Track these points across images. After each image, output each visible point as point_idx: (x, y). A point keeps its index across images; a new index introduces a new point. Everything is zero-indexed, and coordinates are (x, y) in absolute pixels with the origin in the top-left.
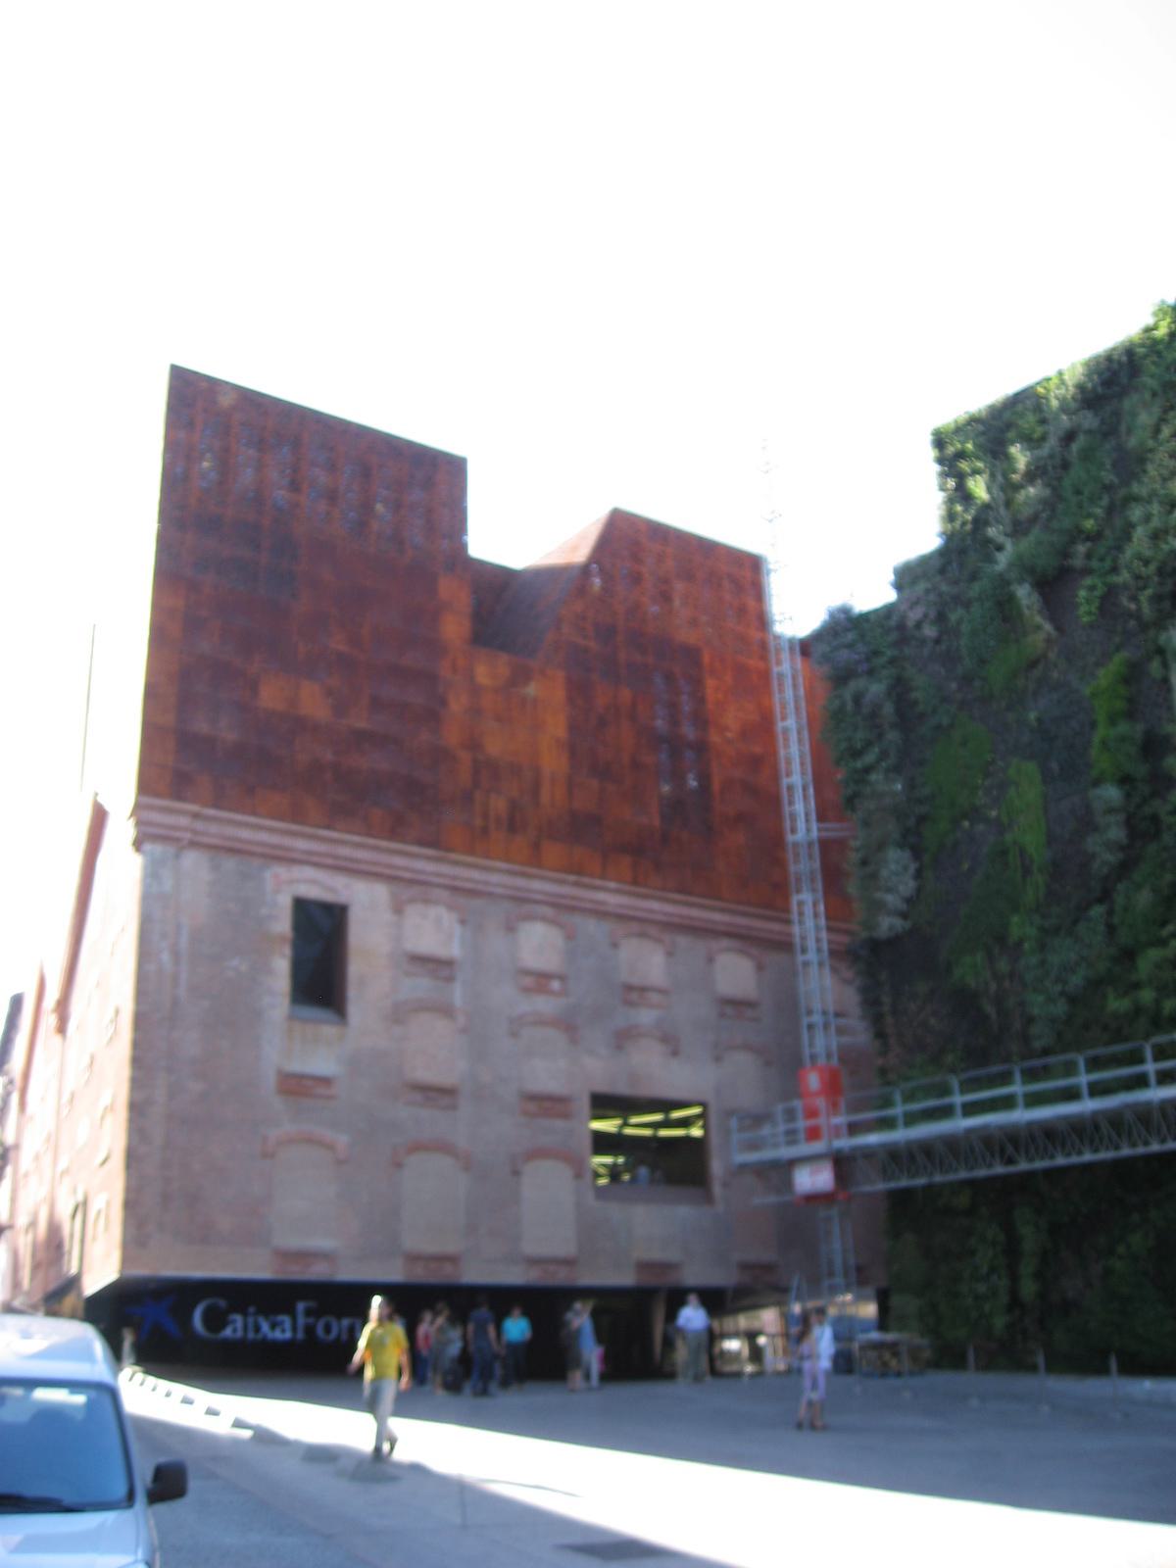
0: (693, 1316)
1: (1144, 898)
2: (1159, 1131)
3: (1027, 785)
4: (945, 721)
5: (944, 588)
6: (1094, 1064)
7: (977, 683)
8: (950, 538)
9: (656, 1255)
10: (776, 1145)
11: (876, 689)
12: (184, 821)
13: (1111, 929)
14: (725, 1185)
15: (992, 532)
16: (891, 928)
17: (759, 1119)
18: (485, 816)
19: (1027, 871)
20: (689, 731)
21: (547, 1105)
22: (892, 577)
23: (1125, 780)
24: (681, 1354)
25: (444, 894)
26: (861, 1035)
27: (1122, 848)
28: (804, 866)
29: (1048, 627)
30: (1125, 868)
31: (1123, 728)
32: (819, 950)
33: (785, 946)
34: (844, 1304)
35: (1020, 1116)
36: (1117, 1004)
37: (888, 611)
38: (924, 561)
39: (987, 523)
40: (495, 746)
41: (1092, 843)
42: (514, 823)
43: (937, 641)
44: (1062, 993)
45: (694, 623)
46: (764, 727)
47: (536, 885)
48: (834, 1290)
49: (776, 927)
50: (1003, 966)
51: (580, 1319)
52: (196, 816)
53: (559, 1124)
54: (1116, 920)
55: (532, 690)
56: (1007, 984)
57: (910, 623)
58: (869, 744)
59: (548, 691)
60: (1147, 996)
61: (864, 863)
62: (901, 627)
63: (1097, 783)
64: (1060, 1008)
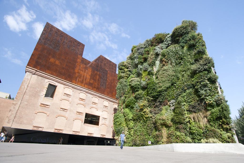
12: (35, 71)
21: (80, 113)
25: (71, 88)
52: (36, 71)
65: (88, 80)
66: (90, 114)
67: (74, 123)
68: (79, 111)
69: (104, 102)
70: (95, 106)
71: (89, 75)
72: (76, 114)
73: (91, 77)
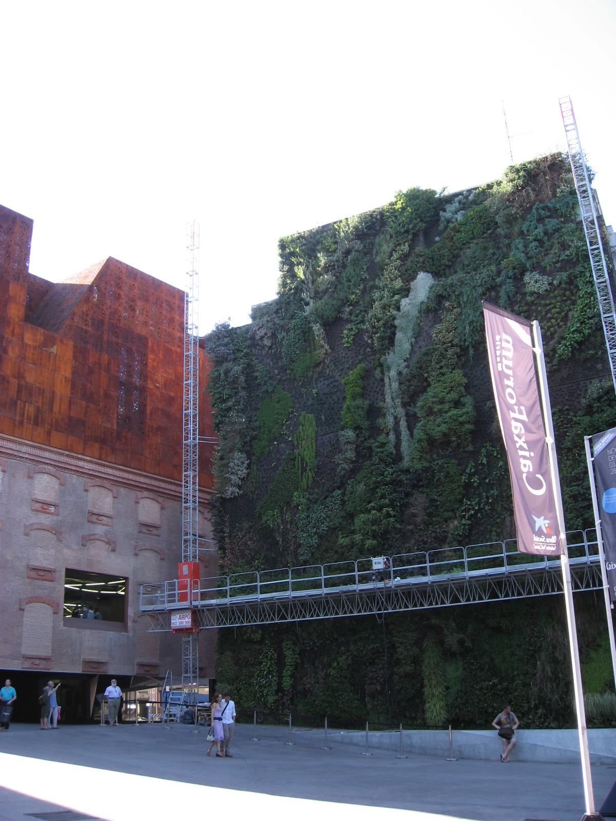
0: (113, 691)
1: (361, 488)
2: (358, 606)
3: (308, 426)
4: (270, 389)
5: (277, 321)
6: (329, 570)
7: (289, 372)
8: (282, 295)
9: (94, 658)
10: (163, 602)
11: (237, 369)
13: (343, 502)
14: (134, 621)
15: (304, 295)
16: (233, 492)
17: (156, 588)
18: (23, 416)
19: (304, 470)
20: (137, 380)
21: (42, 573)
22: (250, 312)
23: (357, 428)
24: (105, 710)
26: (212, 548)
27: (353, 462)
28: (190, 457)
29: (327, 347)
30: (353, 472)
31: (359, 402)
32: (194, 502)
33: (177, 498)
34: (192, 687)
35: (290, 594)
36: (343, 541)
37: (247, 329)
38: (268, 305)
39: (302, 291)
40: (31, 378)
41: (338, 458)
42: (37, 421)
43: (270, 348)
44: (316, 533)
45: (146, 323)
46: (177, 382)
47: (47, 454)
48: (187, 679)
49: (173, 487)
50: (288, 517)
51: (51, 691)
53: (48, 583)
54: (346, 498)
55: (54, 350)
56: (289, 526)
57: (258, 338)
58: (230, 396)
59: (62, 351)
60: (358, 537)
61: (222, 458)
62: (253, 338)
63: (343, 429)
64: (315, 540)
65: (60, 408)
66: (86, 569)
67: (25, 619)
68: (37, 564)
69: (140, 505)
70: (105, 528)
71: (66, 379)
72: (28, 580)
73: (73, 385)
